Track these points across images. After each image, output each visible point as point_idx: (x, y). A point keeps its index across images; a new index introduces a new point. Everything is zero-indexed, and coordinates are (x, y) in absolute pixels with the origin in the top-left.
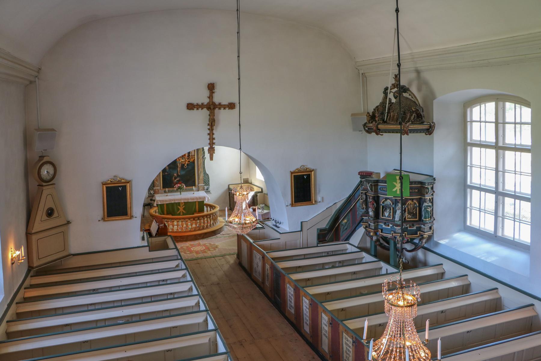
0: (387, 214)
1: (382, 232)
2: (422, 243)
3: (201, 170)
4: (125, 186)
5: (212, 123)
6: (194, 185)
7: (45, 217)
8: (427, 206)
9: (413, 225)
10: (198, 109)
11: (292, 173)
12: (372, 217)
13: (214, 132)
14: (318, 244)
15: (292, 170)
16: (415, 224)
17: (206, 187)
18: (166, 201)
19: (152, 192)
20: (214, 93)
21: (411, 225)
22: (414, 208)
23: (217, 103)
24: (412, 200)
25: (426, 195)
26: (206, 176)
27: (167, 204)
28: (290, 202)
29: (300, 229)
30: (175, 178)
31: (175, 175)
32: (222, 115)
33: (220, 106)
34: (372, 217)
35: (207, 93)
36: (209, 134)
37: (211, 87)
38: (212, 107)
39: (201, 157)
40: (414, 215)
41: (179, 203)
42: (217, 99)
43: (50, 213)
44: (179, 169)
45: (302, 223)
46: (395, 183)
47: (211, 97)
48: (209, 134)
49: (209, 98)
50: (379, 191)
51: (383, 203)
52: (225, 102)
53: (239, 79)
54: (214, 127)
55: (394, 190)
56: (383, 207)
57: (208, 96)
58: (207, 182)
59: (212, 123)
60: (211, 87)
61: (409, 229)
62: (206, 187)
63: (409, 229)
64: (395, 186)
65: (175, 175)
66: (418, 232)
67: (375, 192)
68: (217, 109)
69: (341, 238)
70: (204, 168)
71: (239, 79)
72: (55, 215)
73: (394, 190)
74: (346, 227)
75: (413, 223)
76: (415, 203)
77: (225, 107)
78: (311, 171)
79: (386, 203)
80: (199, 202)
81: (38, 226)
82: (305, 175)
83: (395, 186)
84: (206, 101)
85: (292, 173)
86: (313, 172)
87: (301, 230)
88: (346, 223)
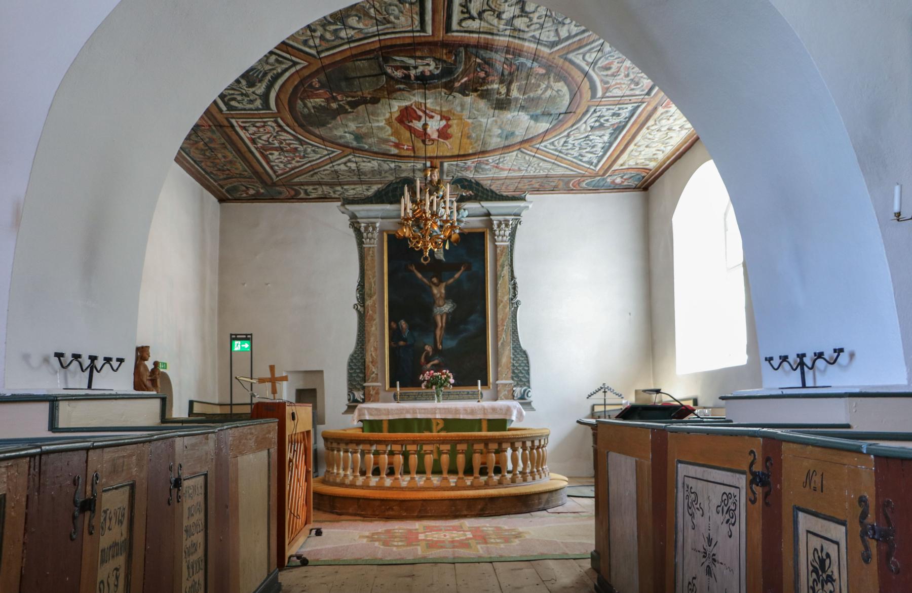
3: (504, 337)
6: (485, 383)
17: (518, 390)
18: (388, 412)
19: (359, 395)
30: (428, 360)
31: (428, 348)
39: (506, 298)
41: (428, 421)
44: (438, 332)
58: (521, 372)
62: (518, 390)
65: (428, 348)
70: (515, 332)
80: (489, 420)
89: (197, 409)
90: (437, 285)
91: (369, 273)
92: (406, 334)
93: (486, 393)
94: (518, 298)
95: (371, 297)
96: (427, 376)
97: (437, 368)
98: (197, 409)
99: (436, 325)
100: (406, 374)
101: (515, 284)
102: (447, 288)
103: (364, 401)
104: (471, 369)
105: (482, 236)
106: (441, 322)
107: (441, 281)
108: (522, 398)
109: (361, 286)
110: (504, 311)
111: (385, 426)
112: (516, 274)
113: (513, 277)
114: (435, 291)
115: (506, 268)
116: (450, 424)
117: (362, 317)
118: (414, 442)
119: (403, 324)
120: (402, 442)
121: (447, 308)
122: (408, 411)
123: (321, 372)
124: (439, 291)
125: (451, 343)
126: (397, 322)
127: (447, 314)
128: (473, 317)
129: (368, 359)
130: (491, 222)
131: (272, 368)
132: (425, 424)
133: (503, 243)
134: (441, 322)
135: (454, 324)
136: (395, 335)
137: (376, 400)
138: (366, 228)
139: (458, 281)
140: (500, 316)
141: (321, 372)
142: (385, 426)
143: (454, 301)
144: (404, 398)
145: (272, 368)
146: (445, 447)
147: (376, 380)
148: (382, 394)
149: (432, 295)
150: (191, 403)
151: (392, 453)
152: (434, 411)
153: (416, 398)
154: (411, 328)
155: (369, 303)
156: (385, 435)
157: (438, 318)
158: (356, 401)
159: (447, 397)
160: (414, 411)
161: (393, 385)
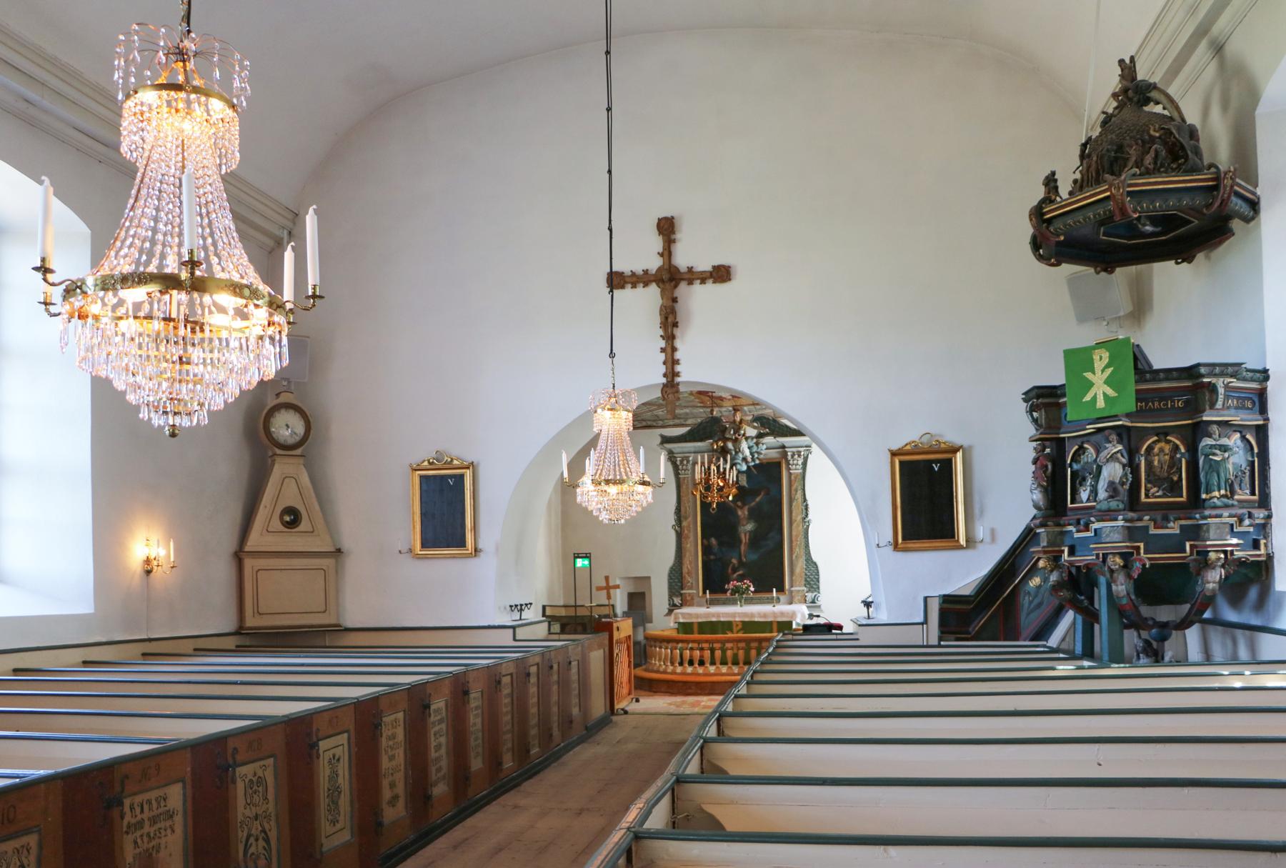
0: (1084, 495)
3: (798, 551)
4: (462, 476)
5: (670, 322)
6: (781, 589)
7: (276, 524)
8: (1212, 447)
10: (634, 286)
11: (894, 454)
13: (678, 343)
14: (940, 639)
15: (895, 447)
18: (697, 616)
19: (677, 601)
20: (674, 241)
21: (1159, 518)
22: (1174, 464)
23: (683, 268)
24: (1163, 433)
26: (812, 566)
27: (700, 624)
28: (889, 536)
29: (921, 619)
30: (734, 570)
31: (734, 561)
32: (697, 298)
33: (693, 276)
35: (657, 243)
36: (663, 350)
37: (667, 228)
38: (670, 278)
39: (799, 518)
40: (1174, 488)
42: (684, 258)
43: (292, 518)
44: (743, 548)
45: (926, 599)
46: (1088, 375)
47: (667, 253)
48: (663, 350)
49: (661, 255)
52: (704, 265)
53: (609, 109)
54: (677, 332)
55: (1088, 398)
56: (1074, 474)
57: (661, 250)
58: (812, 582)
59: (670, 322)
60: (667, 228)
62: (810, 596)
64: (1090, 385)
65: (734, 561)
68: (683, 285)
69: (1024, 633)
70: (807, 546)
71: (609, 109)
72: (305, 525)
73: (1088, 398)
74: (1036, 601)
76: (1176, 448)
77: (703, 278)
78: (955, 450)
79: (1084, 459)
80: (779, 623)
81: (256, 540)
82: (936, 461)
83: (1091, 385)
84: (654, 263)
85: (894, 454)
86: (959, 455)
87: (925, 622)
88: (1039, 587)
89: (548, 612)
90: (741, 508)
91: (684, 499)
92: (716, 549)
93: (782, 598)
94: (810, 517)
95: (686, 518)
96: (731, 586)
97: (741, 578)
98: (548, 612)
99: (740, 541)
100: (716, 584)
101: (807, 508)
102: (749, 510)
103: (681, 606)
104: (769, 578)
105: (778, 465)
106: (745, 539)
107: (744, 504)
108: (813, 602)
109: (678, 511)
110: (798, 529)
111: (696, 628)
112: (808, 497)
113: (805, 500)
114: (740, 513)
115: (800, 492)
116: (749, 626)
117: (679, 536)
118: (706, 641)
119: (713, 541)
120: (698, 642)
121: (750, 527)
122: (713, 615)
123: (649, 578)
124: (743, 513)
125: (754, 557)
126: (708, 539)
127: (750, 532)
128: (771, 535)
129: (685, 570)
130: (785, 454)
131: (607, 578)
132: (727, 626)
133: (796, 470)
134: (745, 539)
135: (756, 540)
136: (707, 550)
137: (691, 605)
138: (681, 462)
139: (759, 504)
140: (794, 533)
141: (649, 578)
142: (696, 628)
143: (756, 521)
144: (712, 603)
145: (607, 578)
146: (742, 645)
147: (691, 588)
148: (696, 600)
149: (738, 517)
150: (544, 607)
151: (702, 649)
152: (734, 615)
153: (724, 603)
154: (721, 544)
155: (684, 524)
156: (696, 636)
157: (743, 536)
158: (675, 605)
159: (750, 601)
160: (718, 615)
161: (704, 592)
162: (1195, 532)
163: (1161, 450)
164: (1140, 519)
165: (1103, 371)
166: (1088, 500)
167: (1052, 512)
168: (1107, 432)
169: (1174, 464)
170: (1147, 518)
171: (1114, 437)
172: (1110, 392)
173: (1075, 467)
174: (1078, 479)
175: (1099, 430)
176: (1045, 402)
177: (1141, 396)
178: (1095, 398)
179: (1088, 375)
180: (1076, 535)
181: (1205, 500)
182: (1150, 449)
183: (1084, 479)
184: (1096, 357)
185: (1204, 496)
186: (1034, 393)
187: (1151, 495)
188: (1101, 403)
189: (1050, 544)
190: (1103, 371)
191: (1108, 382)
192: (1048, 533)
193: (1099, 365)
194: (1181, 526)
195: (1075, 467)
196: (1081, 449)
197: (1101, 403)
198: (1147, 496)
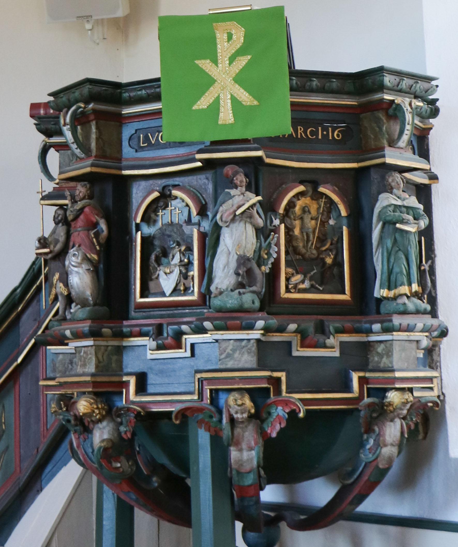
0: (167, 281)
1: (142, 388)
2: (378, 445)
9: (321, 329)
12: (84, 303)
16: (332, 324)
21: (310, 326)
24: (312, 180)
25: (388, 151)
34: (84, 303)
40: (328, 277)
46: (205, 64)
50: (127, 151)
51: (147, 218)
55: (203, 103)
56: (147, 242)
61: (299, 352)
63: (299, 352)
64: (211, 82)
66: (355, 377)
67: (102, 155)
73: (203, 103)
75: (318, 319)
79: (164, 217)
83: (211, 82)
162: (361, 355)
163: (305, 210)
164: (281, 329)
165: (232, 59)
166: (175, 291)
167: (104, 309)
168: (229, 170)
169: (329, 237)
170: (292, 327)
171: (241, 179)
172: (245, 97)
173: (147, 230)
174: (155, 254)
175: (209, 165)
176: (93, 112)
177: (301, 115)
178: (216, 103)
179: (205, 64)
180: (150, 355)
181: (379, 301)
182: (291, 205)
183: (165, 253)
184: (221, 37)
185: (380, 292)
186: (86, 89)
187: (295, 287)
188: (226, 115)
189: (102, 368)
190: (232, 59)
191: (239, 79)
192: (97, 348)
193: (224, 49)
194: (343, 345)
195: (147, 230)
196: (165, 197)
197: (226, 115)
198: (288, 290)
